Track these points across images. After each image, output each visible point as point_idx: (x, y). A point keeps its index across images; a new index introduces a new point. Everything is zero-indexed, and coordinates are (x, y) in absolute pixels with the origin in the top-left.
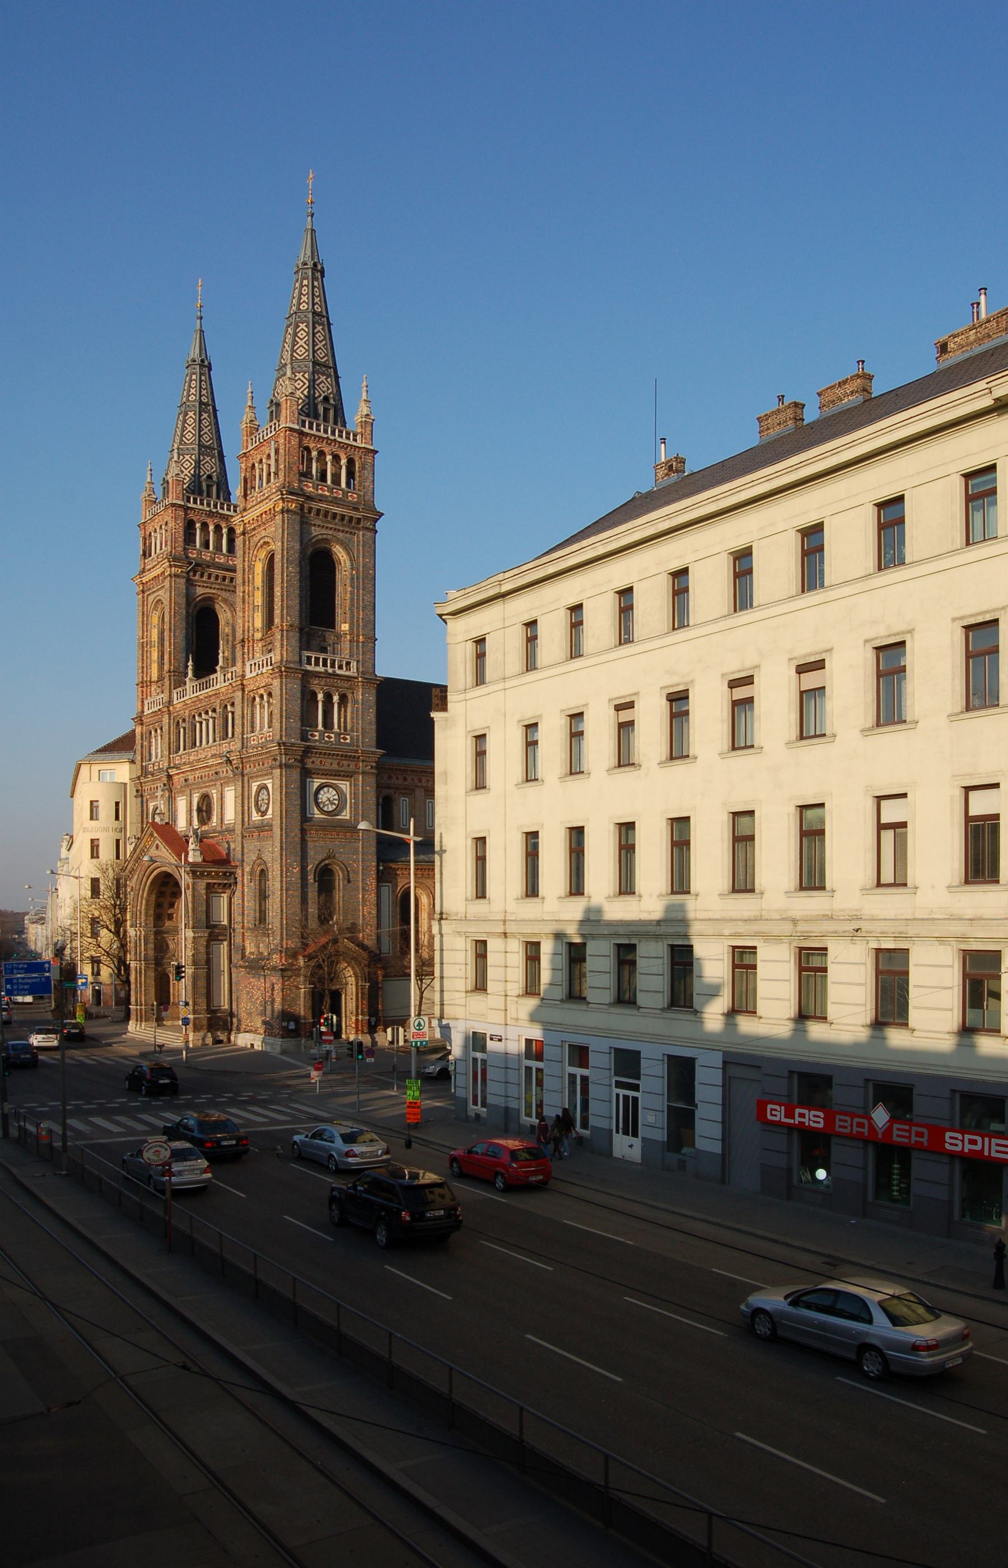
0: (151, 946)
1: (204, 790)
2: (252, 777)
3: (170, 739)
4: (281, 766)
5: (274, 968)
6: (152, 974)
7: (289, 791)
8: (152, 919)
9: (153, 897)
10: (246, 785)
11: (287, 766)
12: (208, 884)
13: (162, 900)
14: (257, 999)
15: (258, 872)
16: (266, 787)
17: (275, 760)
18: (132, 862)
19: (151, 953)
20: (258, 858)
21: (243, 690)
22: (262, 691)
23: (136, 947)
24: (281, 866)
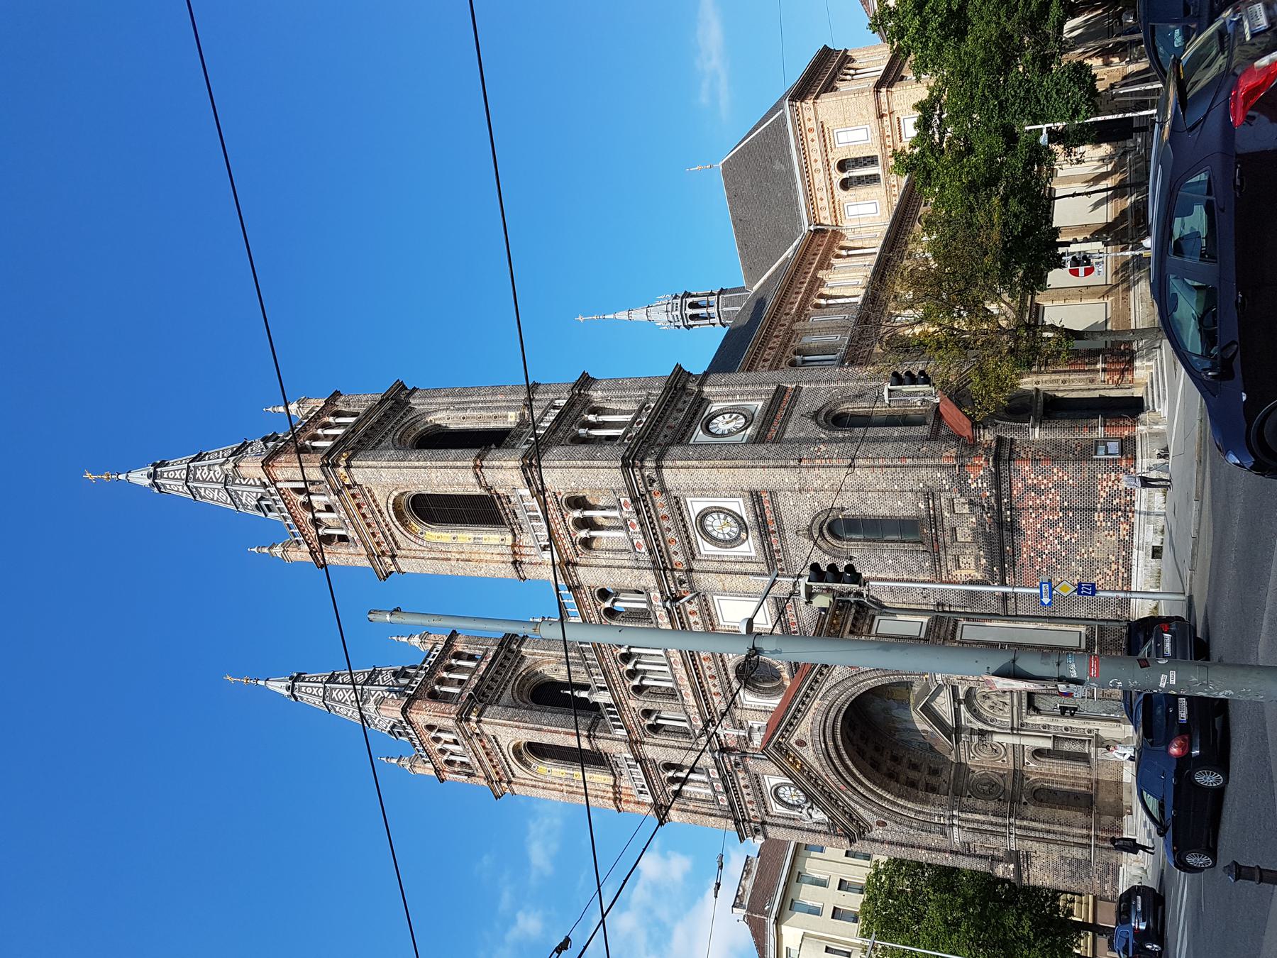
0: (979, 804)
1: (732, 676)
2: (692, 555)
3: (673, 747)
4: (659, 468)
5: (997, 480)
6: (1031, 810)
7: (696, 455)
8: (932, 796)
9: (893, 784)
10: (705, 565)
11: (659, 459)
12: (851, 632)
13: (902, 777)
14: (1059, 538)
15: (834, 542)
16: (703, 516)
17: (652, 481)
18: (835, 811)
19: (991, 805)
20: (811, 537)
21: (576, 564)
22: (569, 521)
23: (980, 831)
24: (813, 467)
